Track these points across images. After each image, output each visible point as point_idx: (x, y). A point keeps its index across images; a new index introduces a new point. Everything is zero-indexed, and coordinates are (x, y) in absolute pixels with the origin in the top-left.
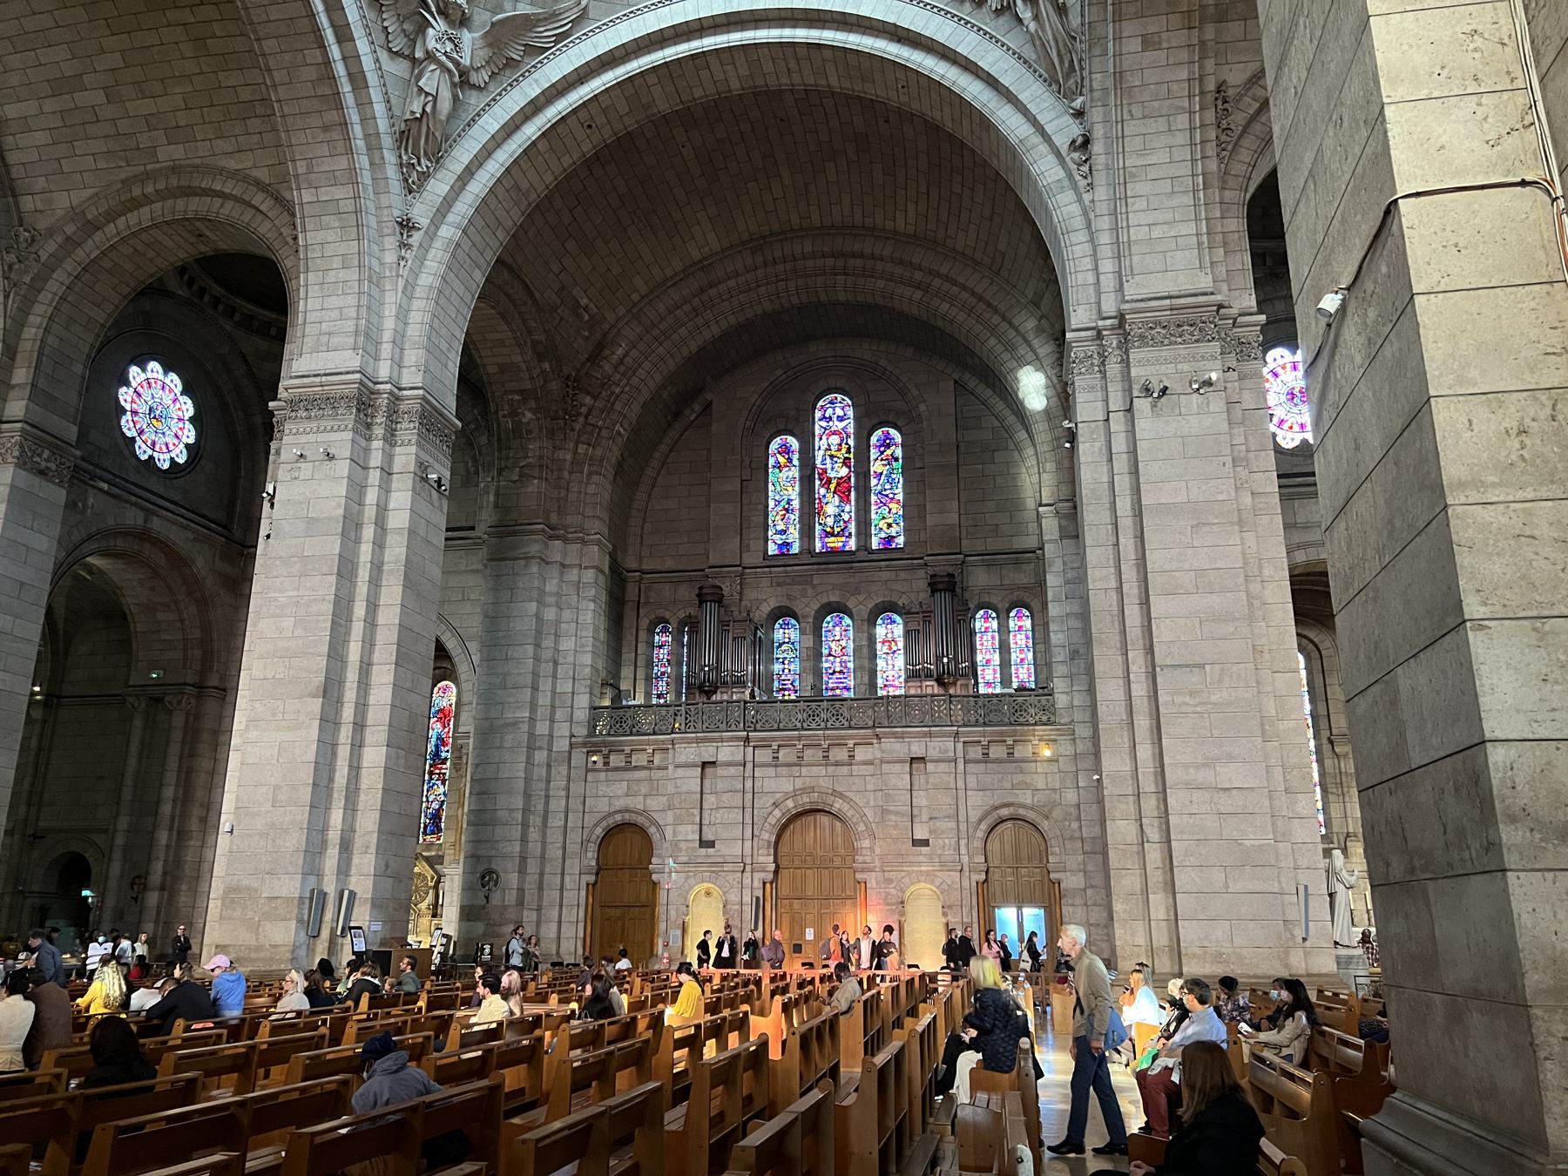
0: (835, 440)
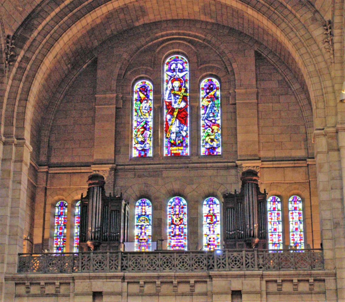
0: (177, 84)
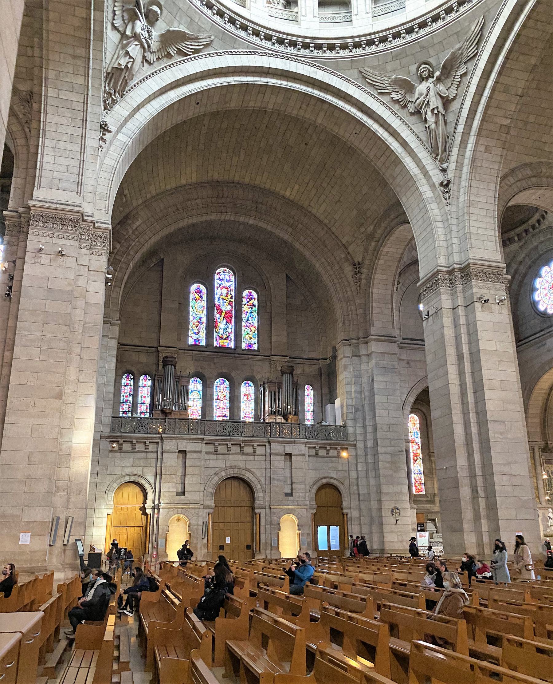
0: (225, 291)
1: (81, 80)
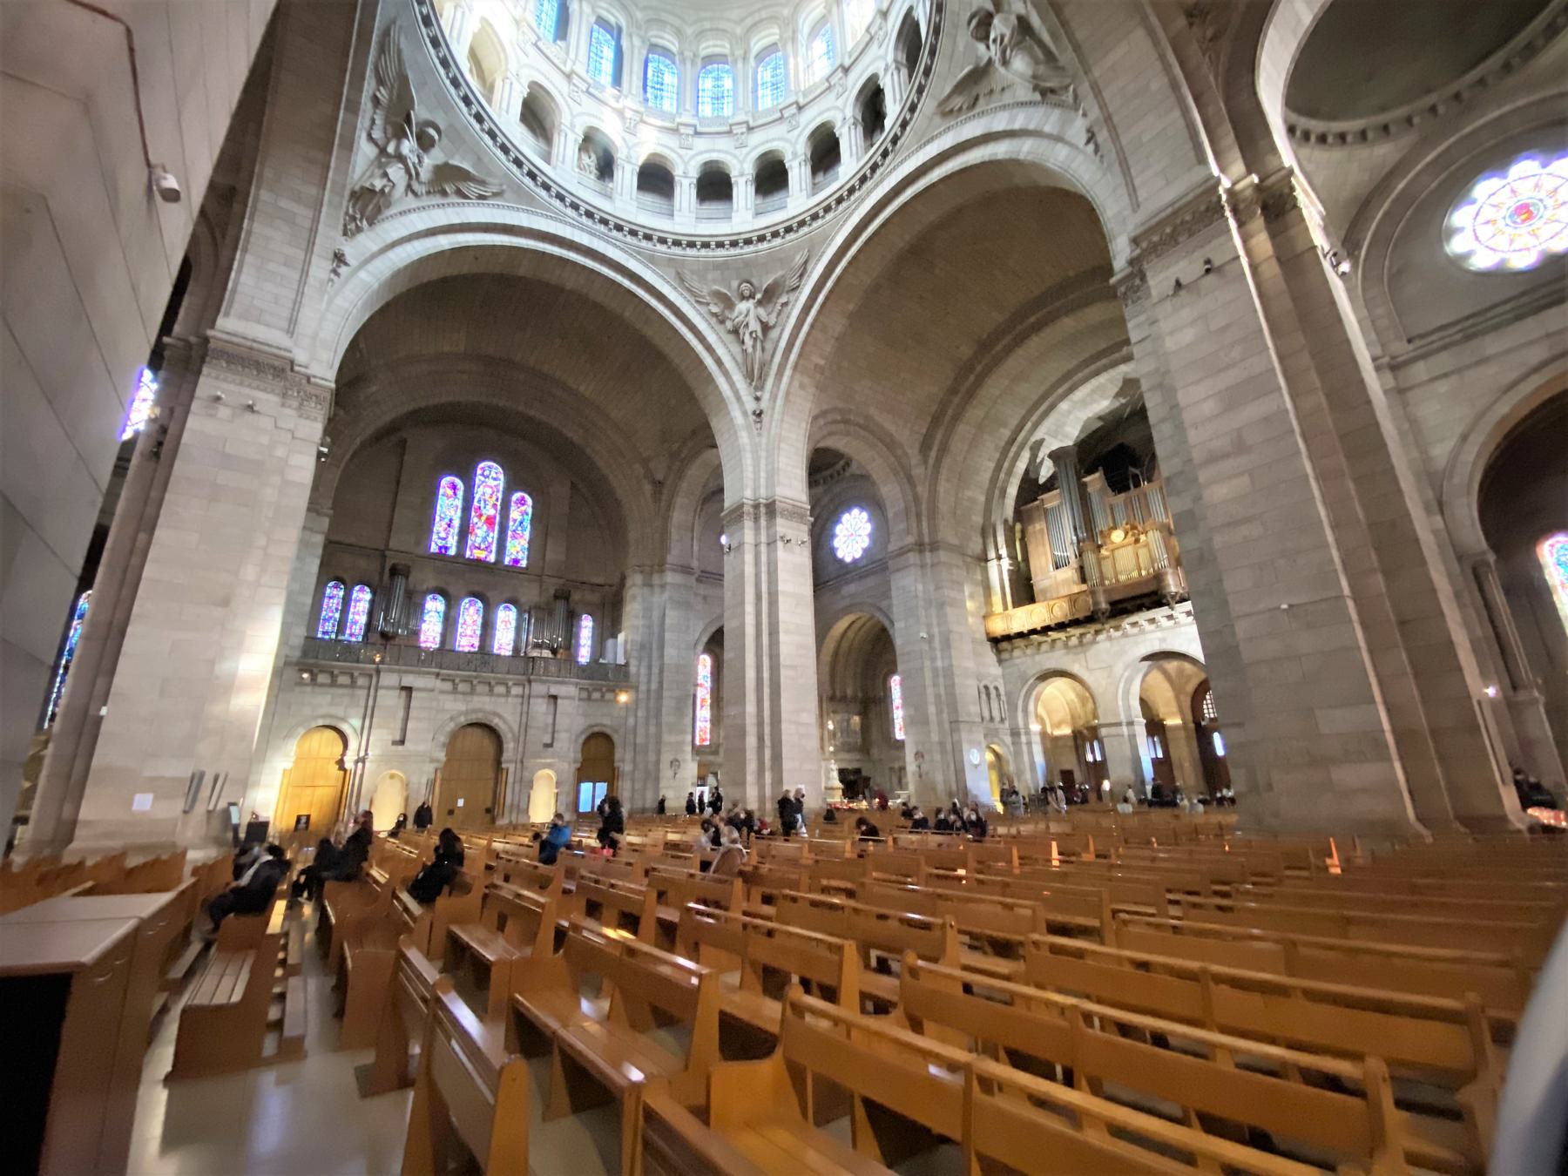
1: (313, 191)
